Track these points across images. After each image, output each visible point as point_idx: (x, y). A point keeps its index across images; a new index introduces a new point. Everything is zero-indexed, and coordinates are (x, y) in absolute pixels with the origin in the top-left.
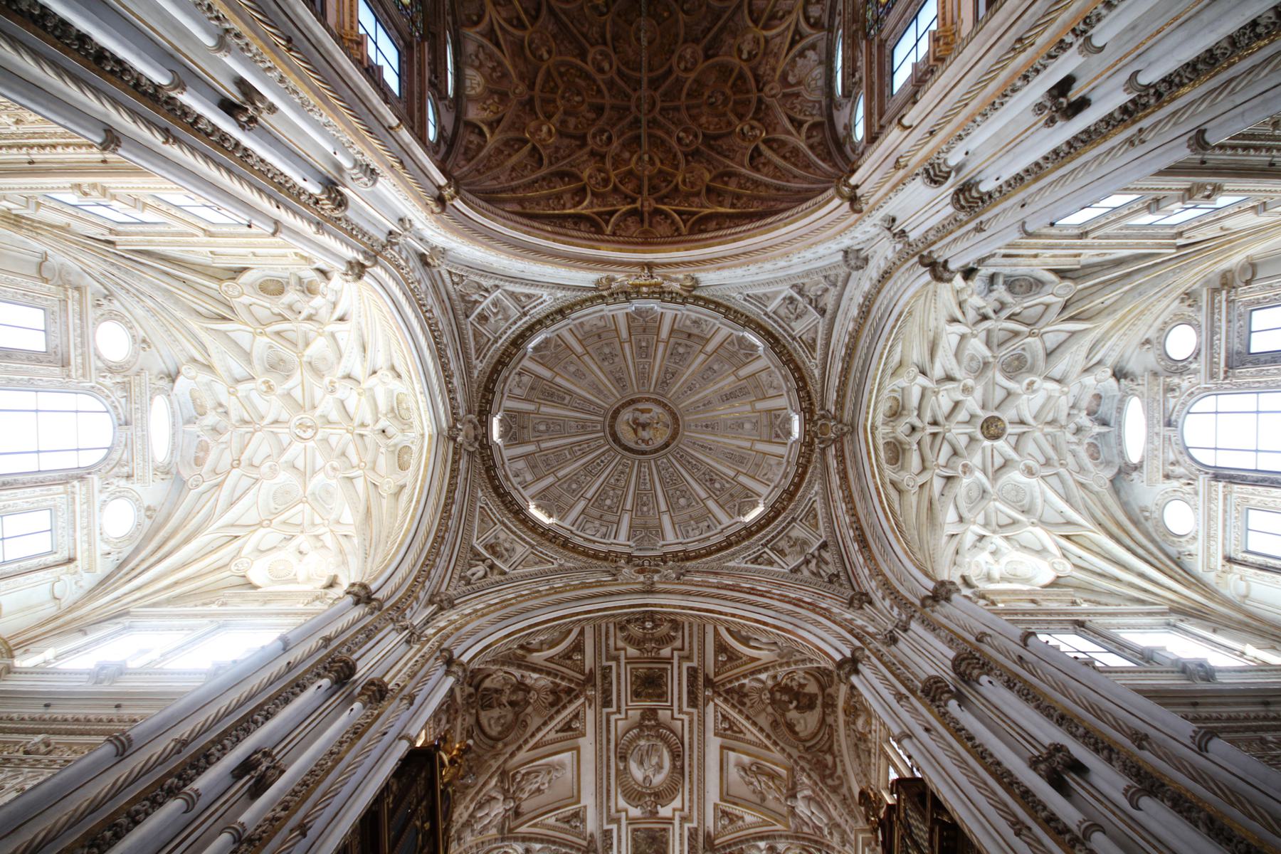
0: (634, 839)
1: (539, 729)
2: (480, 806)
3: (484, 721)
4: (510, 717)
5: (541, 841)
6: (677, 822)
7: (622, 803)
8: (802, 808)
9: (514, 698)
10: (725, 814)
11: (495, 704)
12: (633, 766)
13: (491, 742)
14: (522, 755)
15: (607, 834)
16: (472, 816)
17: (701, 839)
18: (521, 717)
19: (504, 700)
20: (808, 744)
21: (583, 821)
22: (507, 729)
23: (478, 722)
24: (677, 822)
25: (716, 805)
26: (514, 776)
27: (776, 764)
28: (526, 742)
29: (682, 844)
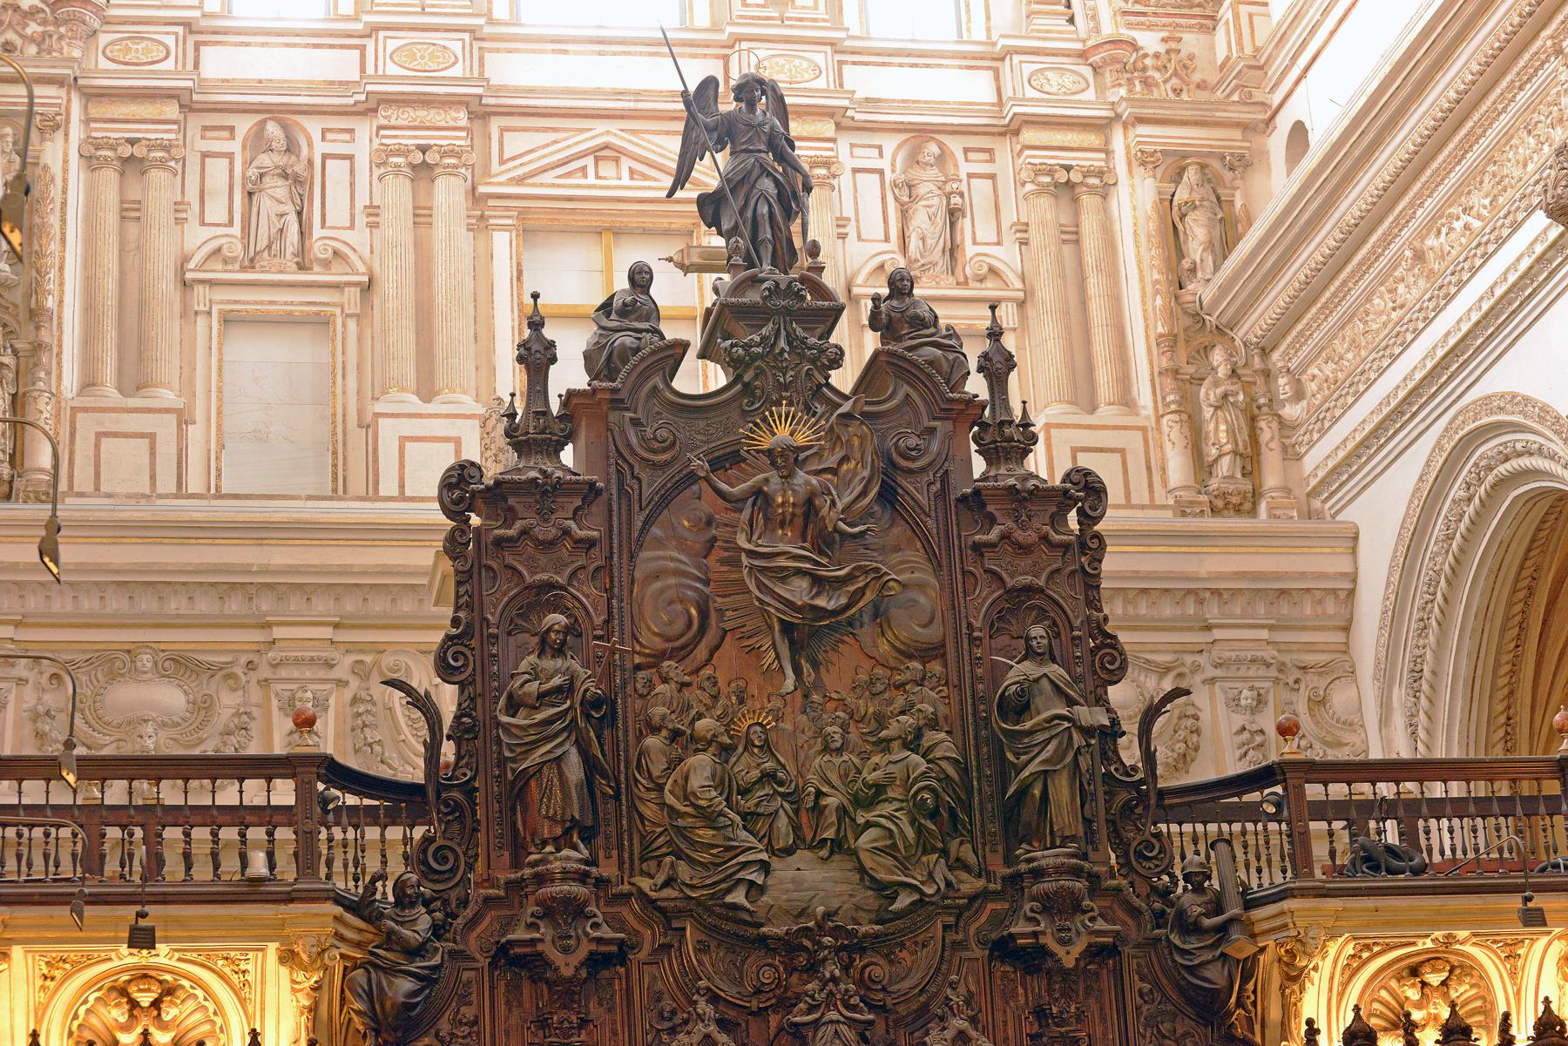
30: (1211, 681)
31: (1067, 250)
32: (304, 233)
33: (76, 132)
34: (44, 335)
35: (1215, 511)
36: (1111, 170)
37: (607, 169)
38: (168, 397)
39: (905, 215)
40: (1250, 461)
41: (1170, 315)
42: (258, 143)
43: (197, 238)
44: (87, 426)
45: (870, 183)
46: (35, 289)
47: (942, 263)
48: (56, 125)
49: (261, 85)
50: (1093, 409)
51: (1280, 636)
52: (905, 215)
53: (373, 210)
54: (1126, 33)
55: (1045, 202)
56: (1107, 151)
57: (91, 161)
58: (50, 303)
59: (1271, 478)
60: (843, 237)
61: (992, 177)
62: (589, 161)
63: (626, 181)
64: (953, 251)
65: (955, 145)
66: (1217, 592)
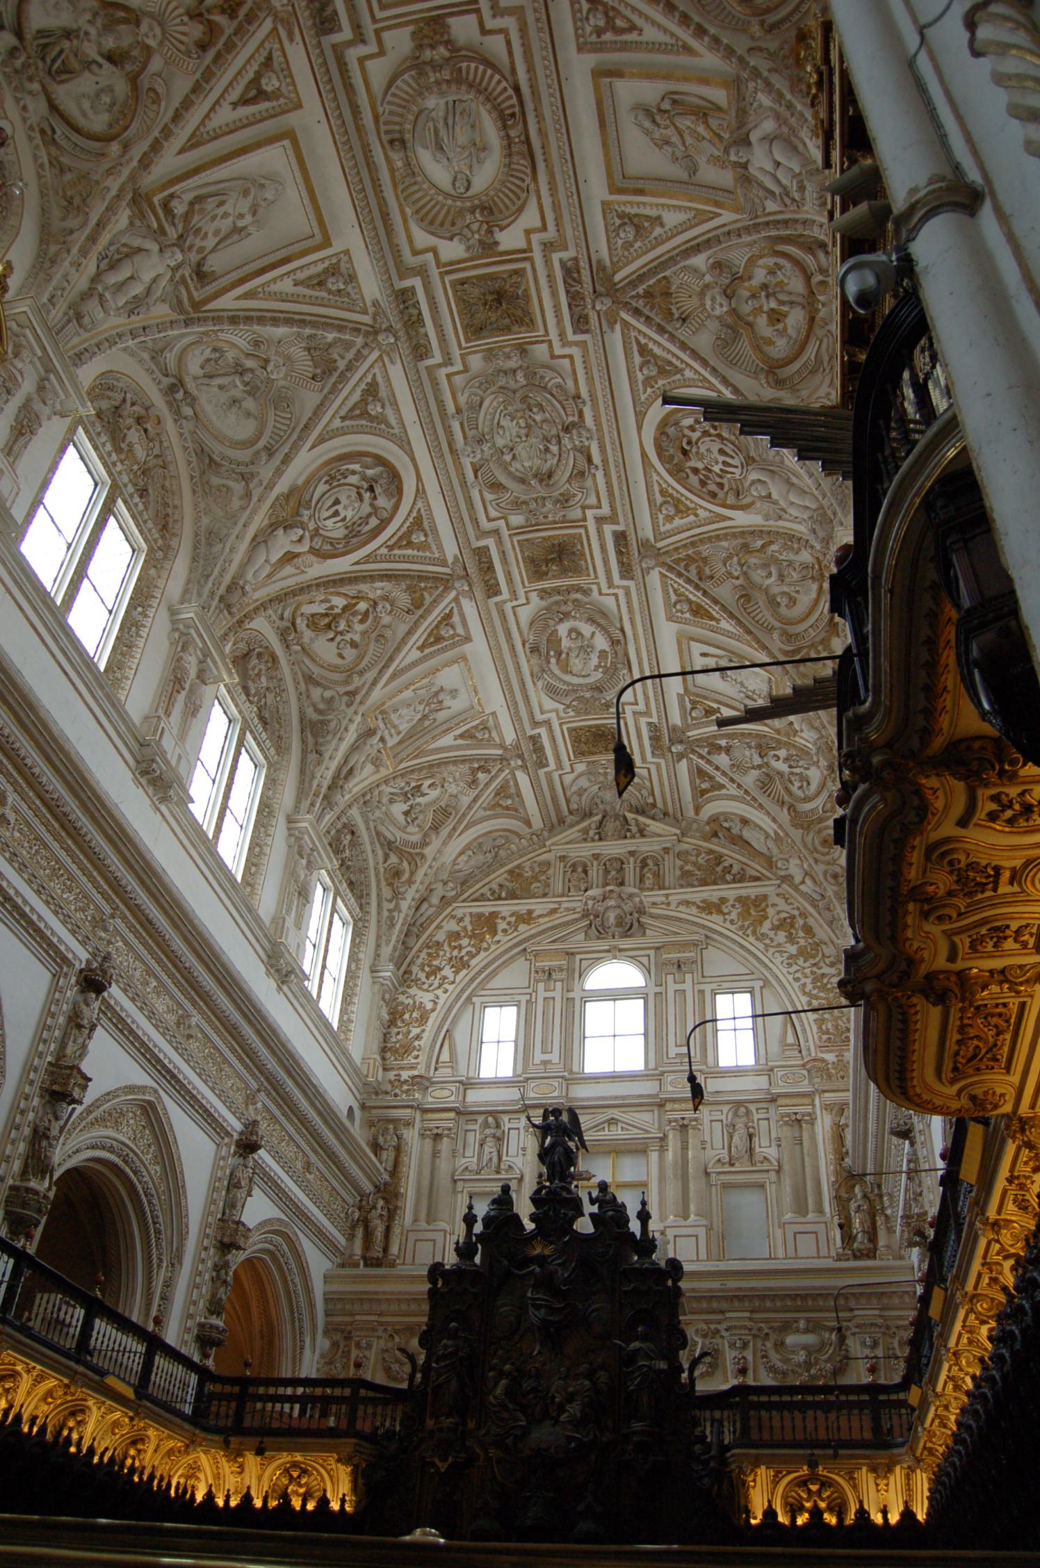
0: (459, 300)
1: (187, 104)
2: (113, 266)
3: (71, 108)
4: (121, 87)
5: (275, 322)
6: (537, 255)
7: (422, 238)
8: (759, 160)
9: (110, 43)
10: (629, 220)
11: (74, 64)
12: (425, 158)
13: (97, 145)
14: (169, 162)
15: (404, 298)
16: (95, 279)
17: (586, 276)
18: (145, 81)
19: (91, 51)
20: (772, 18)
21: (352, 278)
22: (125, 113)
23: (53, 107)
24: (537, 255)
25: (605, 205)
26: (166, 205)
27: (705, 81)
28: (167, 133)
29: (554, 294)
30: (854, 1334)
31: (798, 1147)
32: (500, 1159)
33: (418, 1125)
34: (399, 1204)
35: (856, 1257)
36: (814, 1113)
37: (613, 1128)
38: (443, 1225)
39: (731, 1137)
40: (872, 1236)
41: (837, 1173)
42: (486, 1125)
43: (461, 1162)
44: (412, 1237)
45: (717, 1126)
46: (397, 1185)
47: (747, 1156)
48: (409, 1124)
49: (486, 1104)
50: (805, 1214)
51: (886, 1313)
52: (731, 1137)
53: (524, 1149)
54: (820, 1055)
55: (785, 1128)
56: (814, 1106)
57: (422, 1136)
58: (402, 1190)
59: (882, 1242)
60: (704, 1149)
61: (768, 1119)
62: (606, 1125)
63: (620, 1132)
64: (751, 1150)
65: (752, 1107)
66: (853, 1294)
